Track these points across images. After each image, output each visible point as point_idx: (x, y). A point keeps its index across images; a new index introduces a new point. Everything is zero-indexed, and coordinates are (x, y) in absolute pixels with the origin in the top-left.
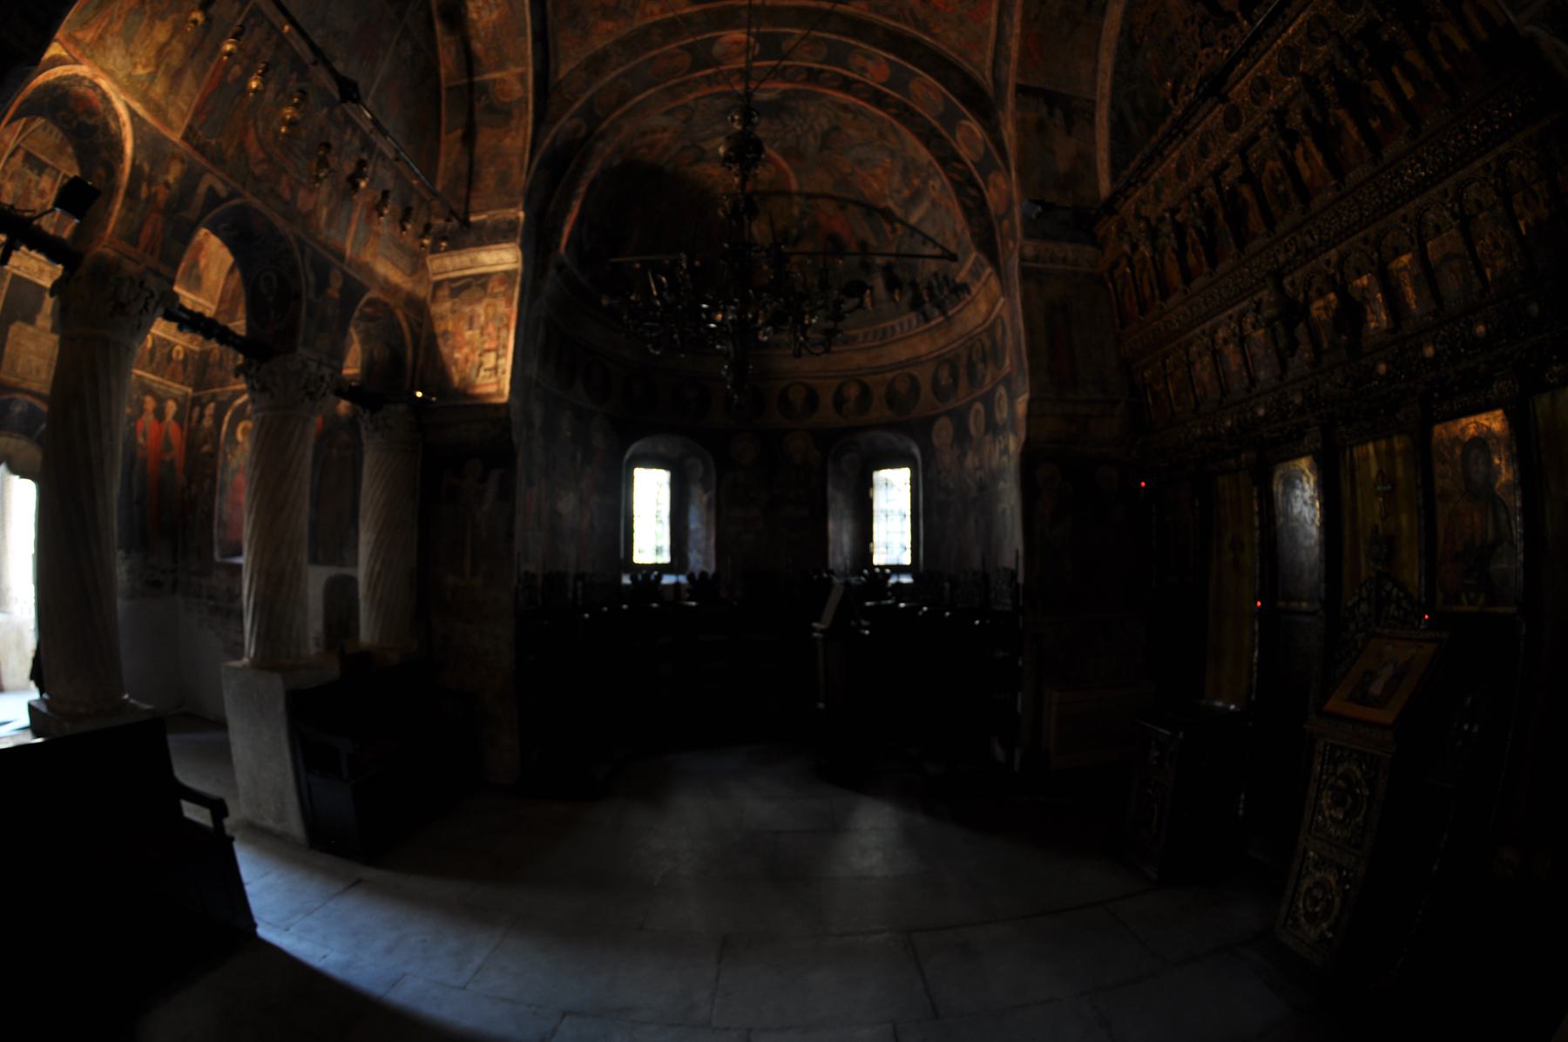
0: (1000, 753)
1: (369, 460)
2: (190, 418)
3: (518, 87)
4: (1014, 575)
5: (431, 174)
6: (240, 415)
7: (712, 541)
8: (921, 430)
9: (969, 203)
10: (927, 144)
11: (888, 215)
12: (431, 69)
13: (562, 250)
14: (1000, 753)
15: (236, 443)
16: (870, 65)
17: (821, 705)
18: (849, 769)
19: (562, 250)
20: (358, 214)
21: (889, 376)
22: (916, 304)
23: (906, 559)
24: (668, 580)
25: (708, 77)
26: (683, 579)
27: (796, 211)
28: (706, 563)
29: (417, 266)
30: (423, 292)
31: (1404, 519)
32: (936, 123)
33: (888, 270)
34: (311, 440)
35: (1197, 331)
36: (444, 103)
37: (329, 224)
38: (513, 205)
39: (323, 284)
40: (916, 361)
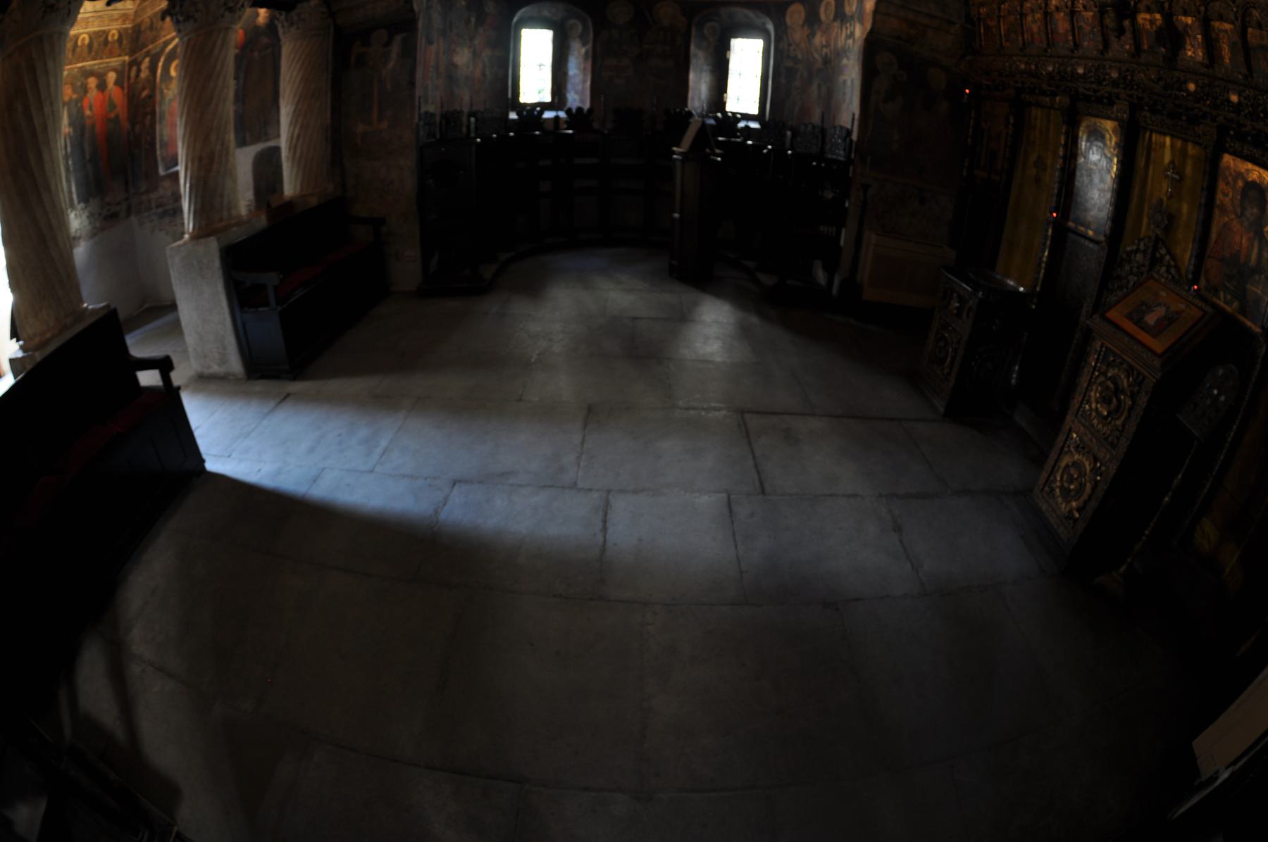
0: (821, 276)
1: (286, 50)
2: (129, 78)
4: (849, 132)
6: (171, 57)
7: (589, 83)
14: (821, 276)
15: (171, 78)
17: (676, 215)
18: (697, 271)
23: (754, 110)
24: (548, 115)
26: (562, 114)
28: (582, 101)
31: (1185, 208)
34: (232, 52)
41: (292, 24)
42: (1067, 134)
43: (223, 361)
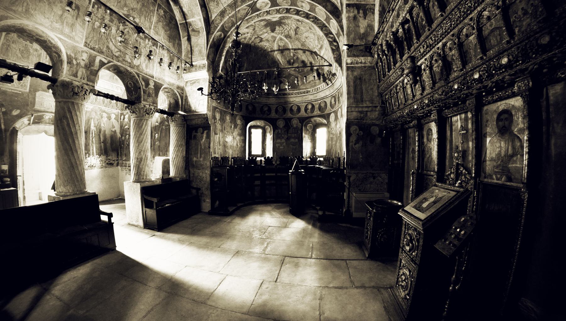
3: (200, 23)
5: (180, 51)
8: (327, 117)
9: (334, 48)
10: (322, 30)
11: (315, 53)
12: (172, 18)
13: (220, 71)
16: (303, 4)
19: (220, 71)
20: (156, 64)
21: (320, 102)
22: (324, 81)
25: (257, 15)
27: (292, 55)
29: (180, 77)
30: (182, 84)
32: (325, 22)
33: (317, 70)
35: (398, 81)
36: (176, 29)
37: (147, 66)
38: (203, 59)
39: (147, 84)
40: (326, 97)
41: (173, 121)
42: (419, 135)
43: (137, 221)
